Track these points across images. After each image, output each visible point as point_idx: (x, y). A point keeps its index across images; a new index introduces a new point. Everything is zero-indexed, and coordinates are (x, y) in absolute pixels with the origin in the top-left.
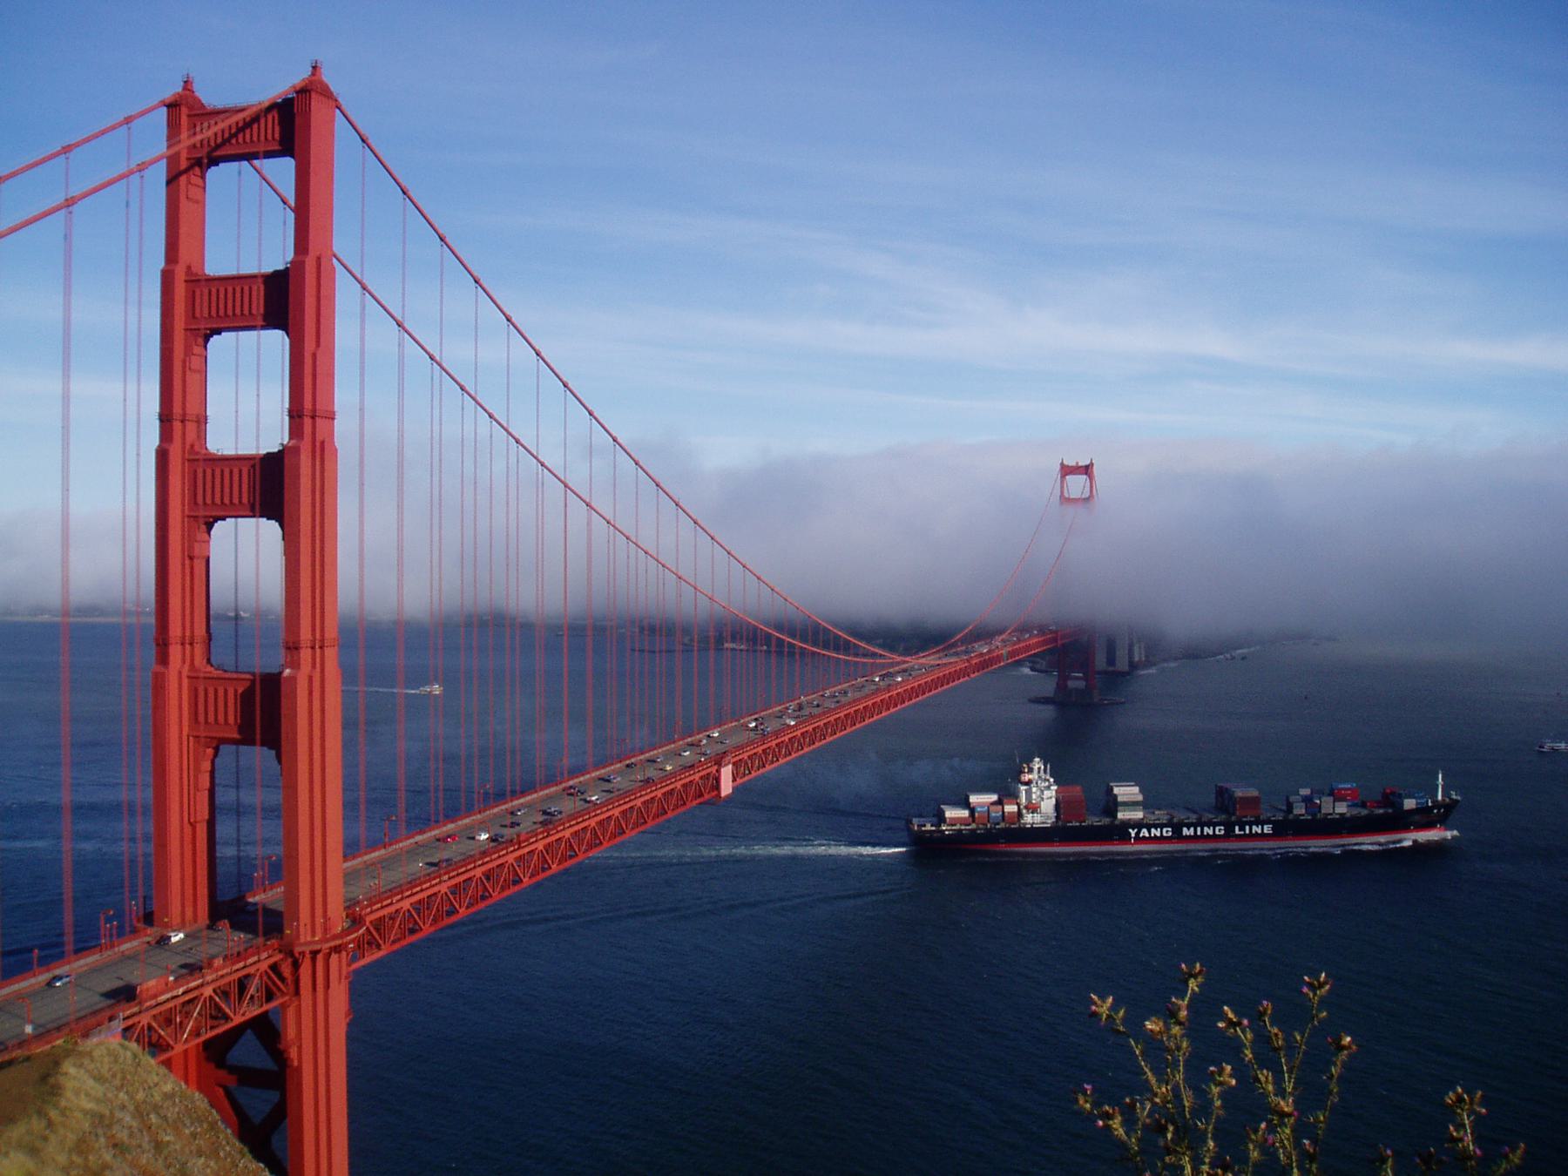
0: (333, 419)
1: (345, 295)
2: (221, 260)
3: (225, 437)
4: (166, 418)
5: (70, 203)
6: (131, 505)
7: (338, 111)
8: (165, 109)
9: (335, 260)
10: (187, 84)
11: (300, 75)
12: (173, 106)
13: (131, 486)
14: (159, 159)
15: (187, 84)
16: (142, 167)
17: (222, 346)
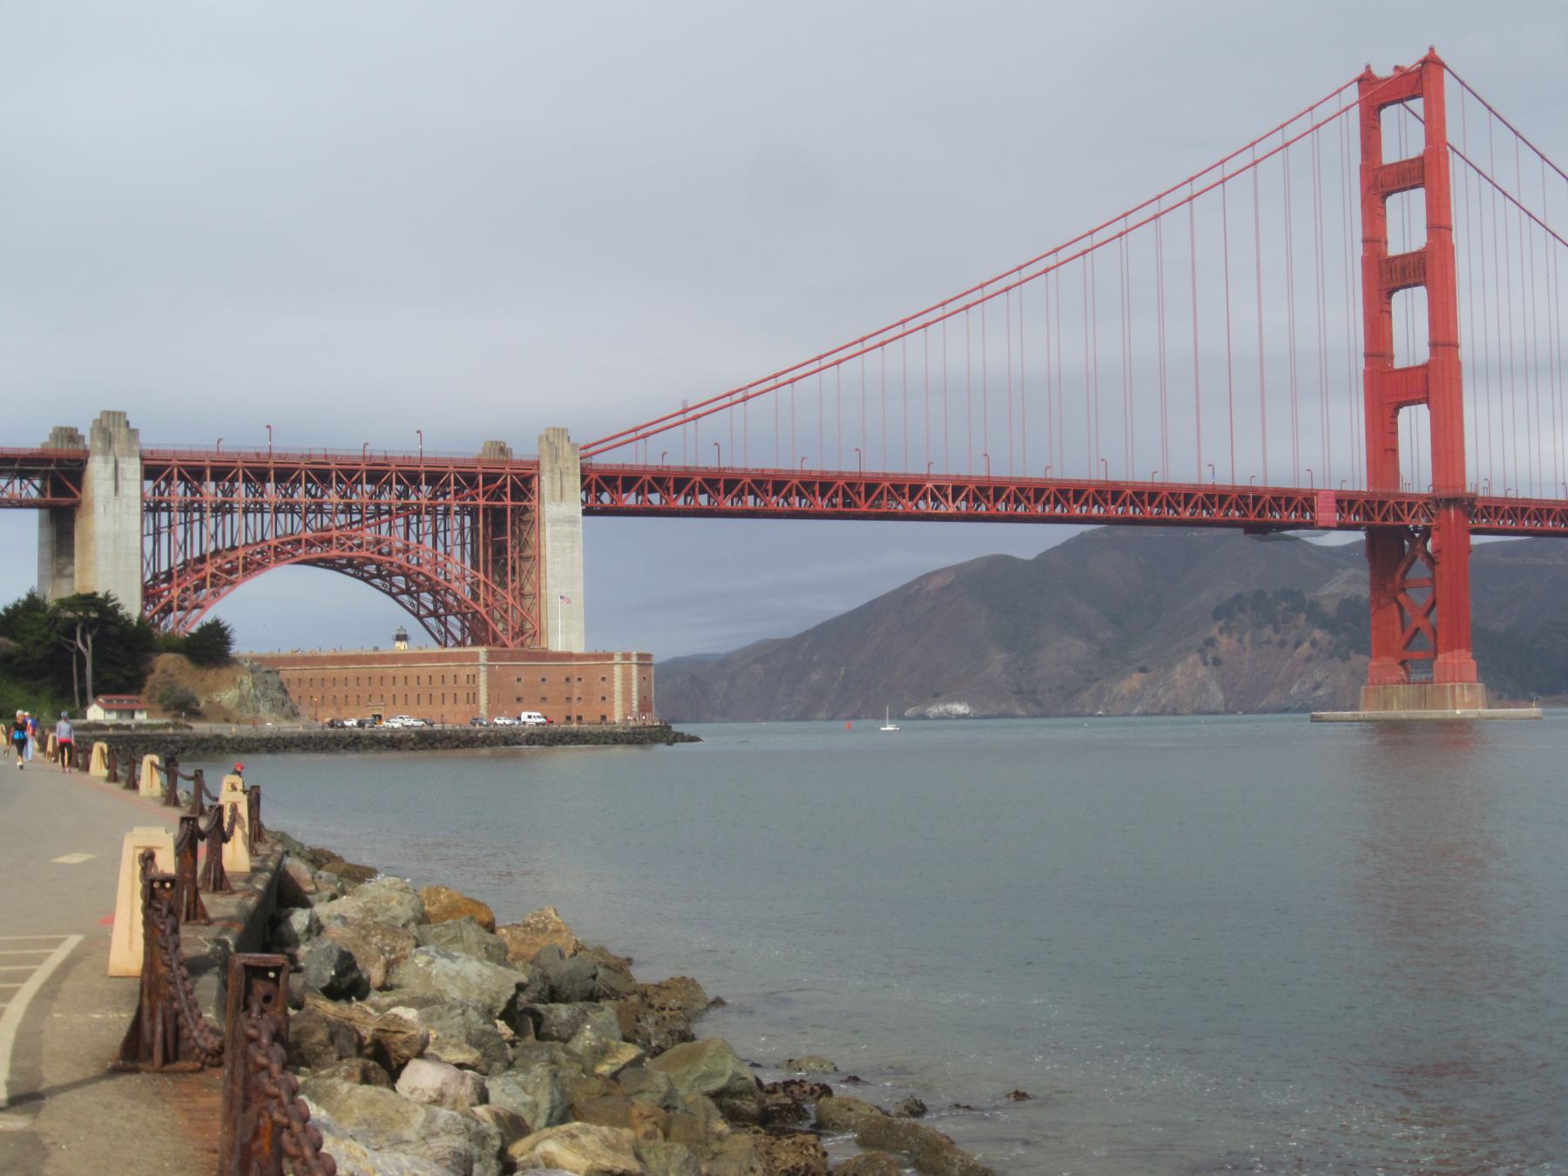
0: (1451, 230)
1: (1456, 165)
2: (1391, 154)
3: (1395, 248)
4: (1366, 241)
5: (1318, 127)
6: (1352, 340)
7: (1445, 70)
8: (1356, 83)
9: (1448, 148)
10: (1368, 67)
11: (1424, 53)
12: (1360, 80)
13: (1355, 432)
14: (1354, 104)
15: (1368, 67)
16: (1347, 109)
17: (1393, 202)
